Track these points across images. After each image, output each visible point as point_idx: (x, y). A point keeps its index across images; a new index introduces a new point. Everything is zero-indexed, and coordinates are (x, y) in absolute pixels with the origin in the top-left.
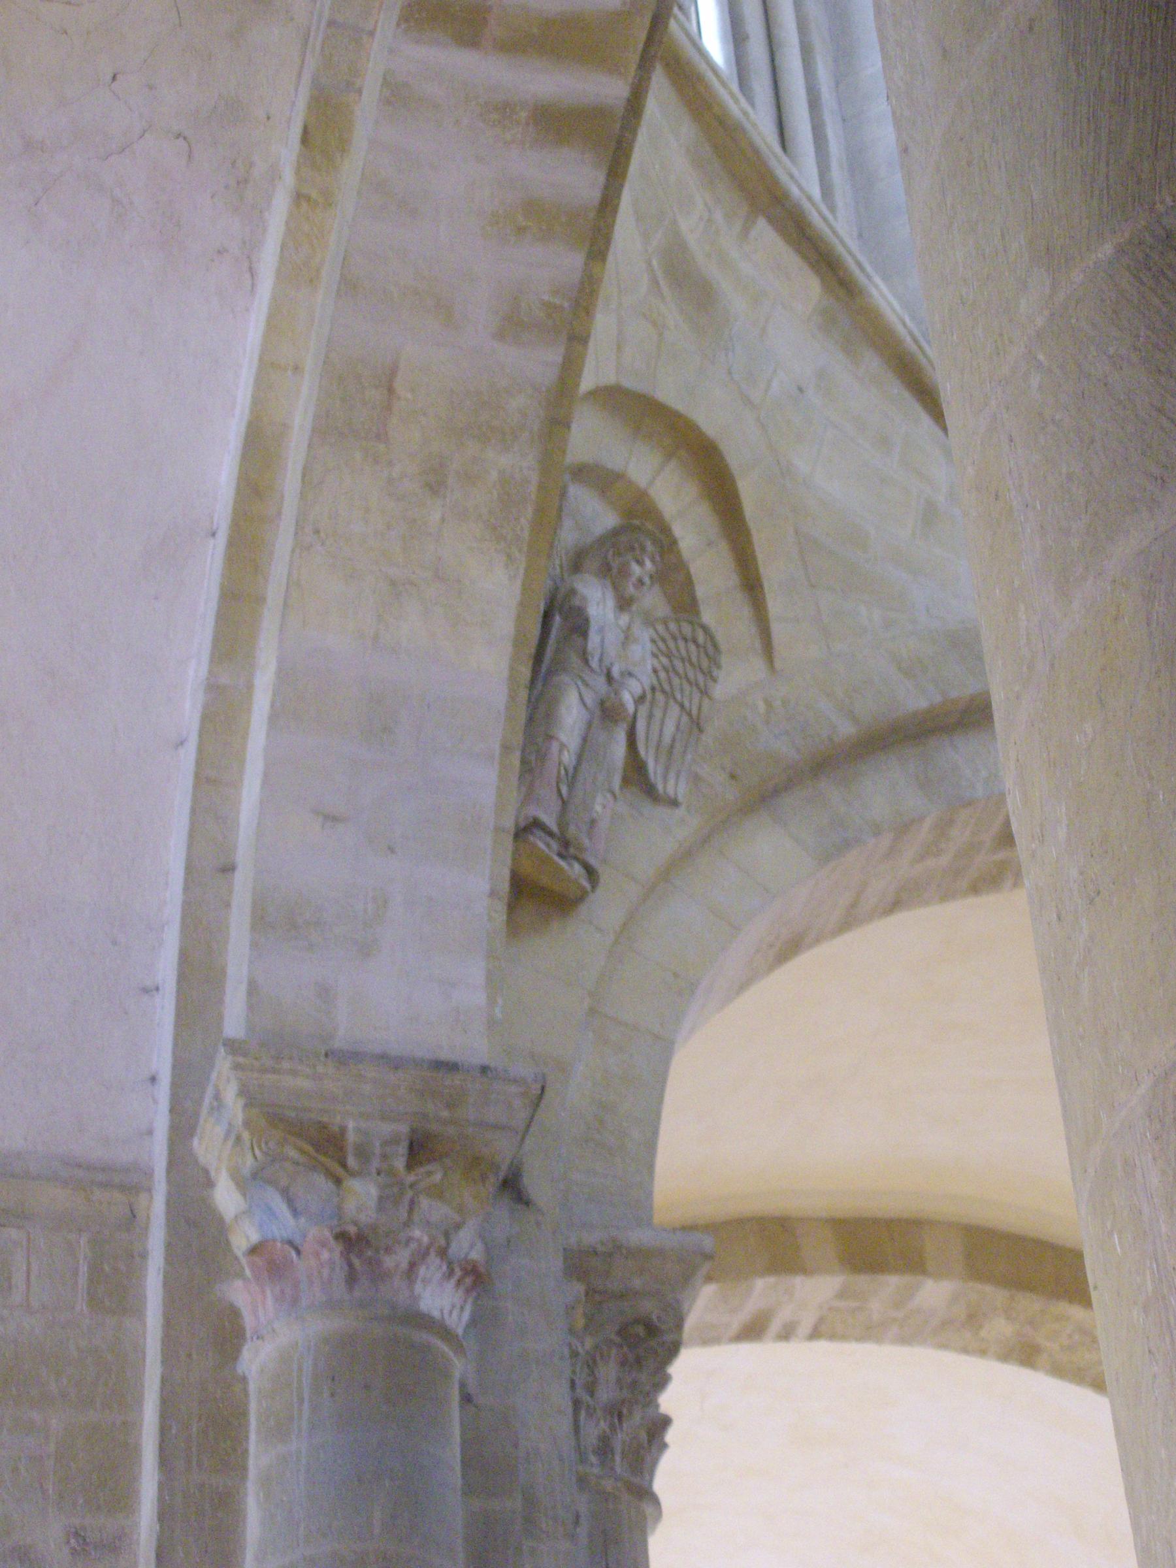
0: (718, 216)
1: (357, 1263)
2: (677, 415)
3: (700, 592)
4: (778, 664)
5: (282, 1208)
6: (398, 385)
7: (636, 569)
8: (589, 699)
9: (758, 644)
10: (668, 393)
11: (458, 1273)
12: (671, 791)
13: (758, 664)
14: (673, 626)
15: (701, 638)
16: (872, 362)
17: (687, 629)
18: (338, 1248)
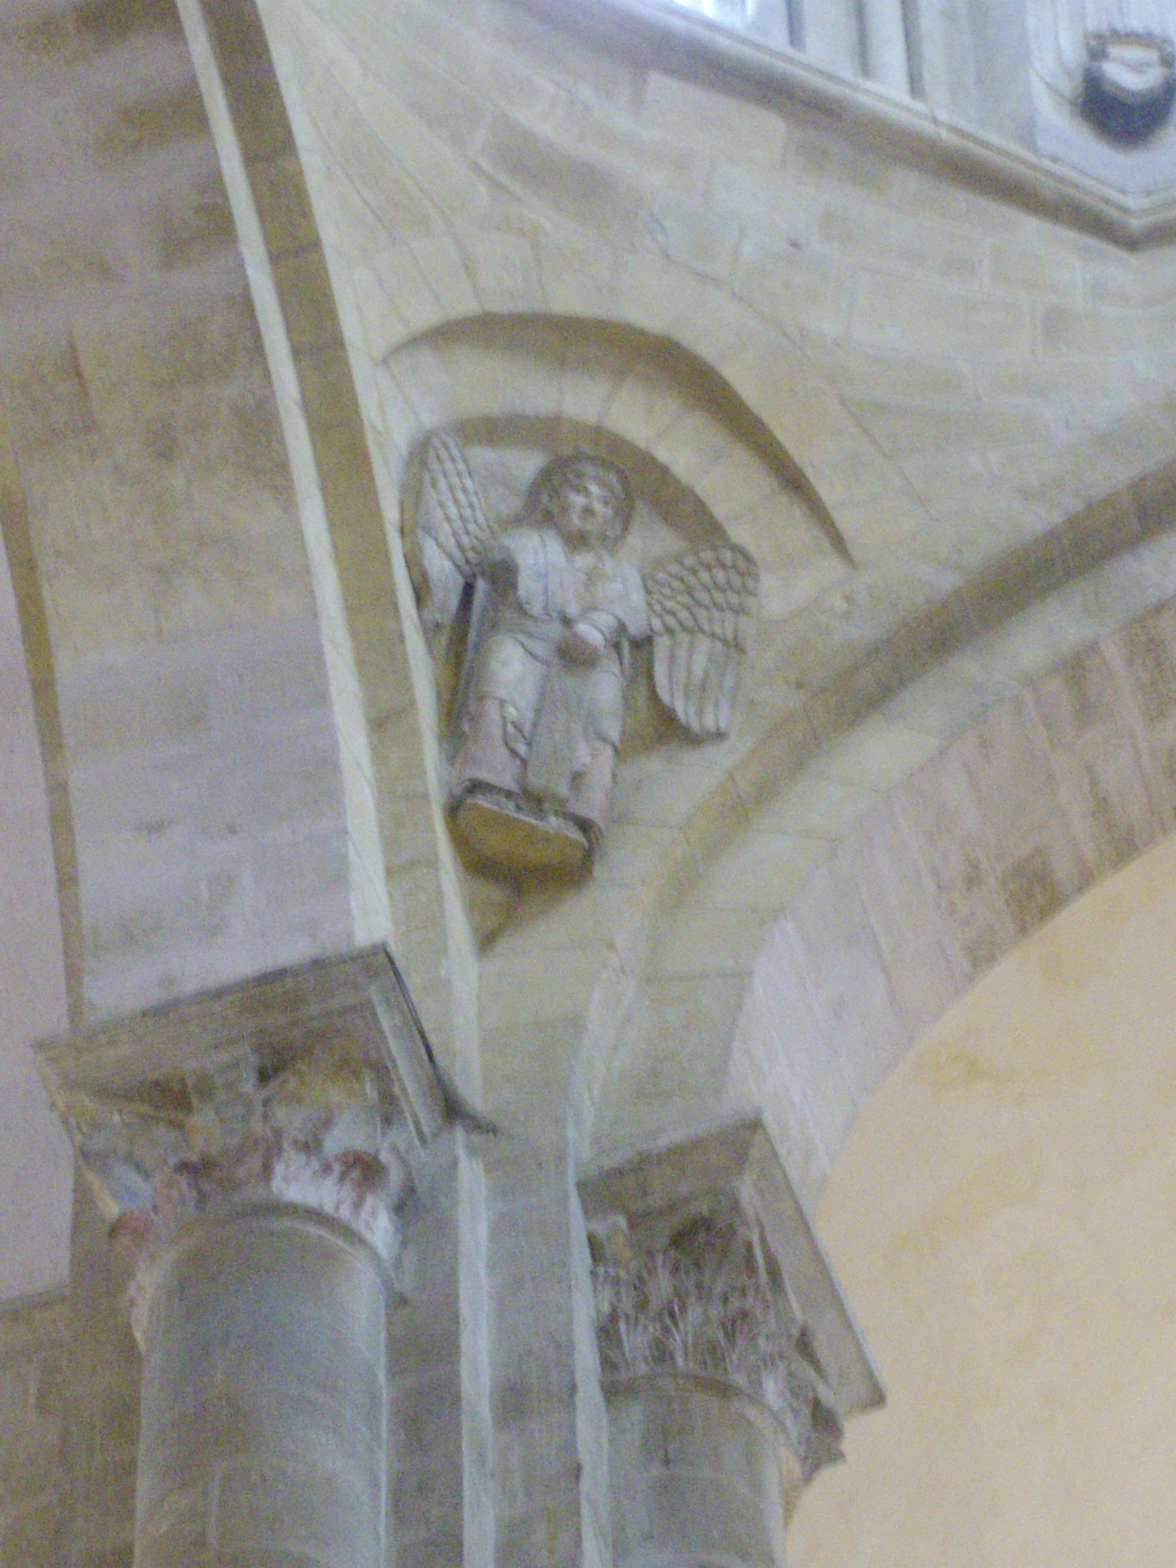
0: (586, 92)
1: (207, 1187)
2: (601, 325)
3: (719, 511)
4: (855, 553)
5: (135, 1180)
6: (87, 366)
7: (578, 500)
8: (539, 648)
9: (826, 545)
10: (569, 298)
11: (337, 1168)
12: (709, 722)
13: (831, 567)
14: (690, 561)
15: (728, 556)
16: (908, 182)
17: (708, 556)
18: (183, 1180)
